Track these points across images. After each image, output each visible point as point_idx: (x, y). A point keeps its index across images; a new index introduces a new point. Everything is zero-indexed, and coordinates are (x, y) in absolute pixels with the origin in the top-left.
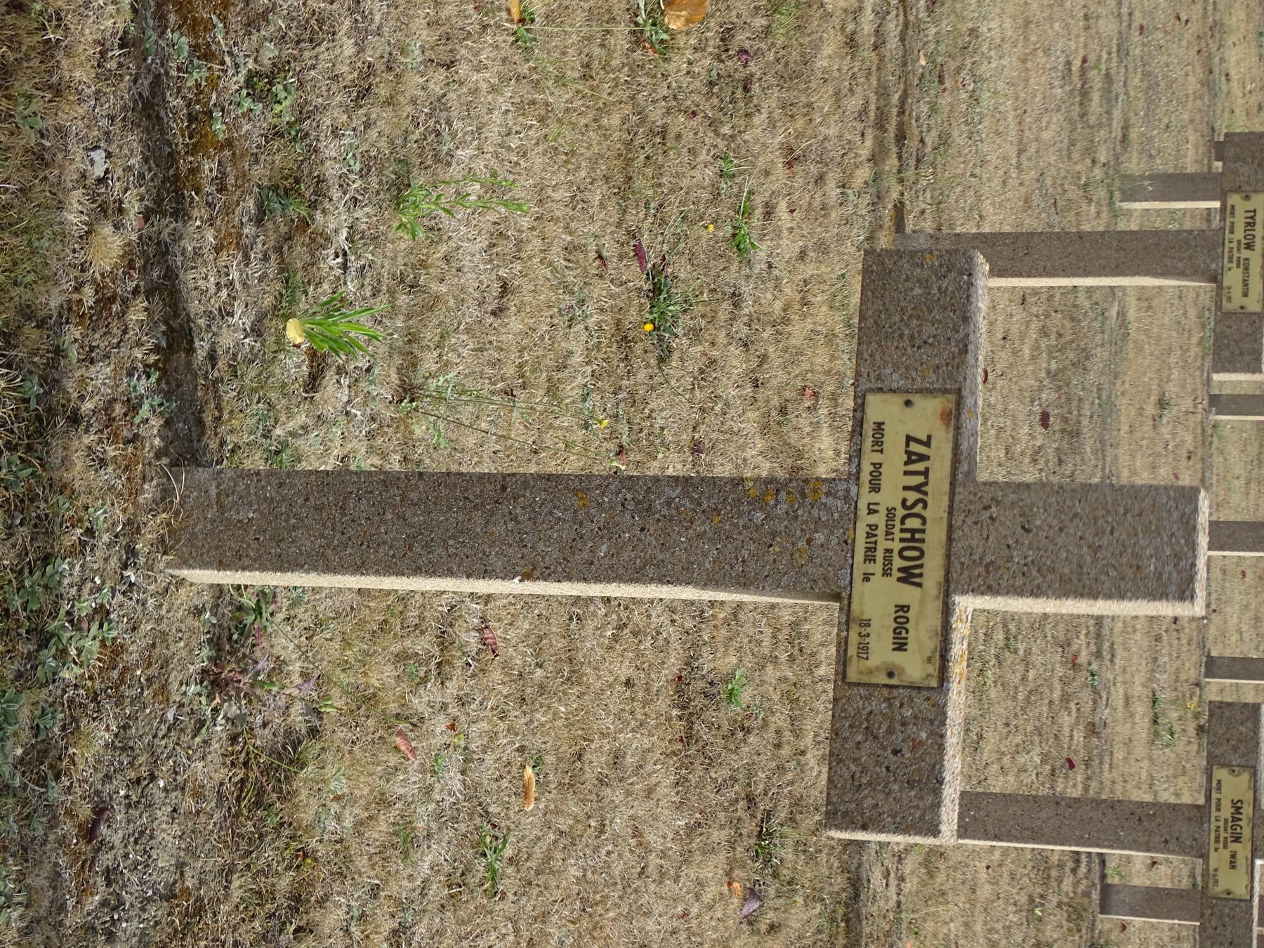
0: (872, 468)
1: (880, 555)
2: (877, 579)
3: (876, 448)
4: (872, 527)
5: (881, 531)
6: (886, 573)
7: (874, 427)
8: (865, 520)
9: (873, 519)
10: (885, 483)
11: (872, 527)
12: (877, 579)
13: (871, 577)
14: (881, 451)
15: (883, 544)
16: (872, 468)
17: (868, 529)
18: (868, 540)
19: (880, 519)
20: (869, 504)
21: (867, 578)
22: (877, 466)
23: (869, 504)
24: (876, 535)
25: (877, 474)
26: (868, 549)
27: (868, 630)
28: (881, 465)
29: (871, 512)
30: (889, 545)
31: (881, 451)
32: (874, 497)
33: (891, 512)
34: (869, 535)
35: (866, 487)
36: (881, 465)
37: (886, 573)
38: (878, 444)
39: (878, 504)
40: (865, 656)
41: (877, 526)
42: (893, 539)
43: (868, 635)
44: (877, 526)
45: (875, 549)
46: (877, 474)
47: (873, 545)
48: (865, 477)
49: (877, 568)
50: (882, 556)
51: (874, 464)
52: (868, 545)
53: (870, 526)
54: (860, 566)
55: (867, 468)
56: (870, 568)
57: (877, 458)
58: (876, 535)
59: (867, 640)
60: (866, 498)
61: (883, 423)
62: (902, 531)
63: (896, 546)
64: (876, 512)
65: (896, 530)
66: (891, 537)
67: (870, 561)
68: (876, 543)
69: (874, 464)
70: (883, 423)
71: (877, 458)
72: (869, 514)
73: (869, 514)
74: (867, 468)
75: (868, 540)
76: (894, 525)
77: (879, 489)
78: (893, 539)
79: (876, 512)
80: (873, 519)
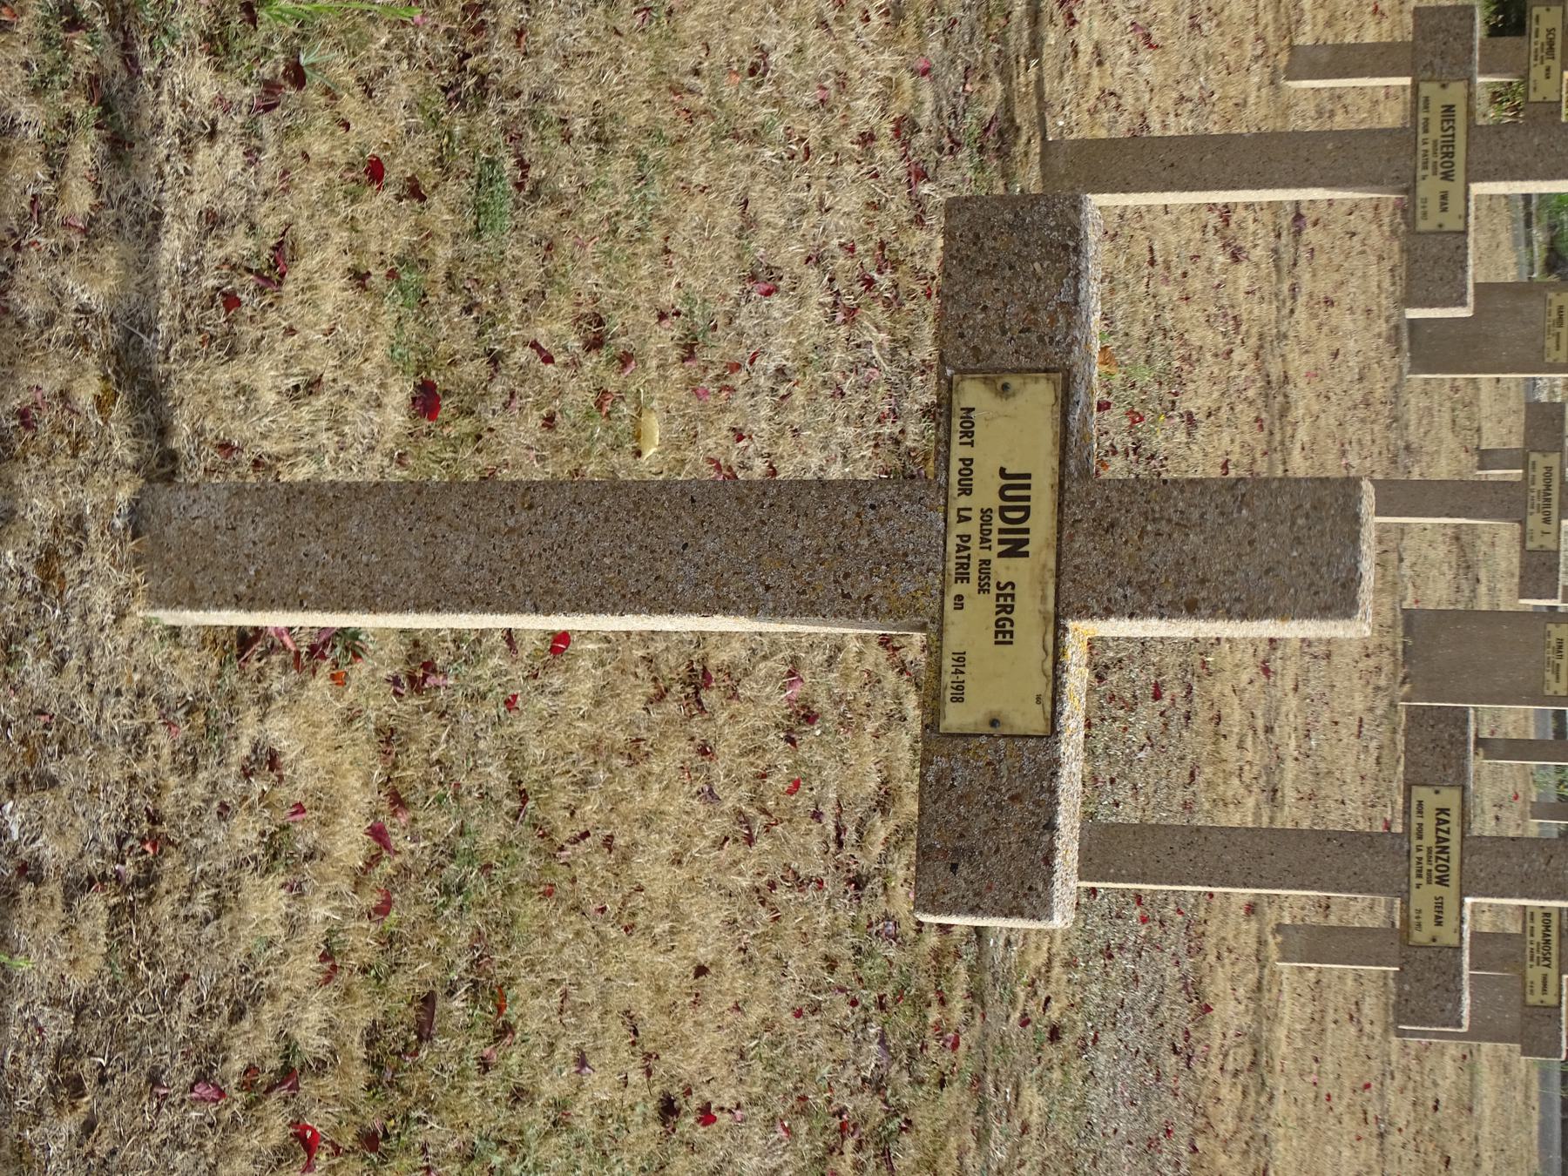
9: (962, 528)
11: (965, 538)
14: (972, 444)
16: (961, 465)
22: (967, 462)
32: (963, 501)
34: (960, 549)
38: (968, 433)
48: (954, 477)
57: (965, 452)
62: (1001, 542)
64: (968, 519)
71: (965, 452)
74: (956, 465)
79: (968, 519)
80: (962, 528)
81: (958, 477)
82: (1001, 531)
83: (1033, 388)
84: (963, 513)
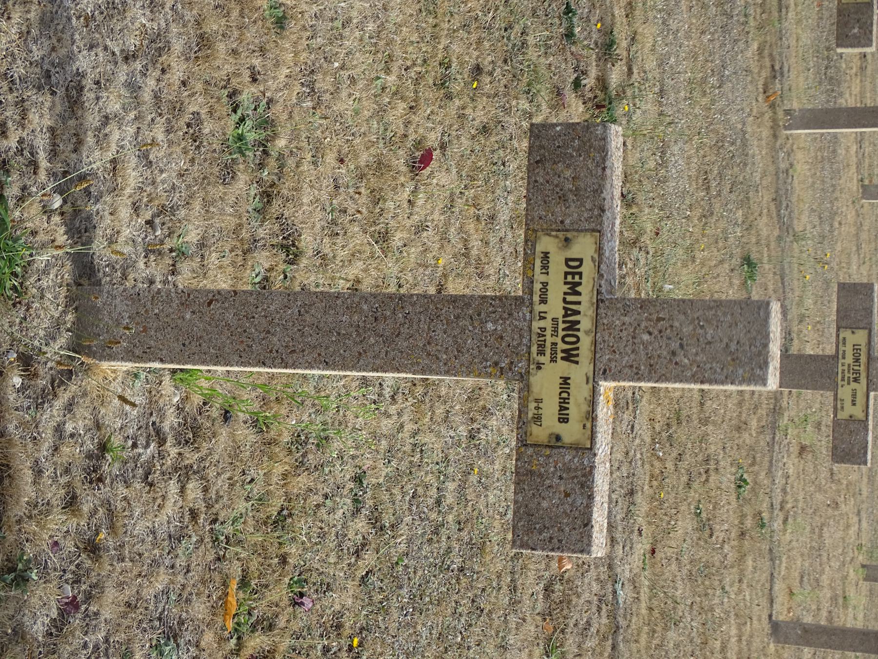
0: (541, 286)
3: (544, 271)
6: (553, 360)
7: (542, 255)
9: (542, 324)
10: (551, 296)
13: (541, 366)
14: (547, 273)
16: (541, 286)
17: (539, 331)
20: (540, 312)
24: (545, 336)
25: (545, 290)
26: (539, 346)
28: (547, 283)
29: (542, 318)
30: (554, 339)
32: (543, 307)
35: (536, 298)
37: (553, 360)
38: (545, 267)
39: (546, 312)
41: (545, 328)
42: (557, 336)
44: (545, 328)
46: (545, 290)
47: (543, 343)
50: (550, 347)
52: (539, 343)
53: (540, 328)
55: (537, 286)
56: (542, 359)
57: (543, 278)
58: (545, 336)
59: (540, 411)
61: (549, 253)
63: (558, 340)
64: (545, 318)
68: (545, 341)
70: (549, 253)
71: (543, 278)
72: (539, 320)
73: (539, 320)
74: (537, 286)
80: (542, 324)
81: (540, 293)
84: (542, 315)
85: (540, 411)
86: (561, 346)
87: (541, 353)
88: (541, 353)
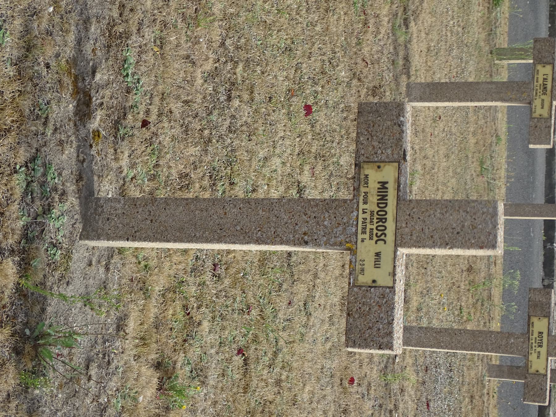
0: (364, 194)
1: (368, 230)
2: (367, 241)
3: (365, 185)
4: (365, 219)
5: (368, 220)
6: (371, 238)
8: (361, 216)
9: (365, 216)
11: (365, 219)
12: (367, 241)
14: (368, 187)
15: (369, 226)
16: (364, 194)
18: (363, 224)
19: (367, 216)
20: (363, 209)
21: (363, 241)
22: (366, 193)
23: (363, 209)
24: (366, 222)
26: (363, 228)
27: (364, 263)
29: (364, 213)
30: (372, 227)
31: (368, 187)
32: (365, 206)
33: (372, 213)
36: (367, 192)
38: (367, 183)
40: (363, 273)
41: (366, 219)
42: (373, 224)
43: (364, 264)
44: (366, 219)
45: (366, 228)
48: (361, 198)
49: (367, 236)
51: (365, 192)
53: (363, 219)
54: (360, 237)
56: (364, 236)
59: (363, 267)
60: (362, 206)
61: (368, 175)
63: (374, 227)
64: (366, 212)
65: (375, 221)
66: (372, 223)
67: (364, 233)
68: (366, 226)
69: (365, 192)
70: (368, 175)
75: (363, 224)
76: (373, 218)
77: (367, 203)
78: (373, 224)
79: (366, 212)
80: (365, 216)
82: (377, 219)
83: (387, 167)
84: (365, 211)
85: (363, 267)
86: (375, 231)
87: (364, 232)
88: (364, 232)
